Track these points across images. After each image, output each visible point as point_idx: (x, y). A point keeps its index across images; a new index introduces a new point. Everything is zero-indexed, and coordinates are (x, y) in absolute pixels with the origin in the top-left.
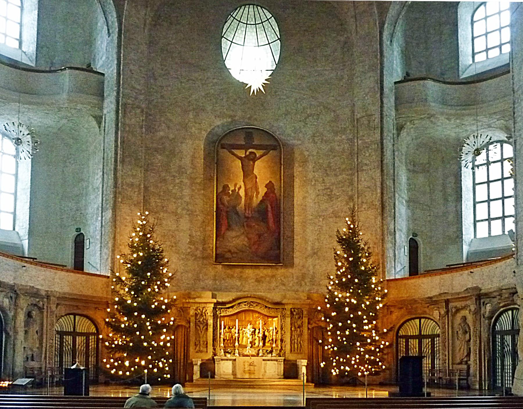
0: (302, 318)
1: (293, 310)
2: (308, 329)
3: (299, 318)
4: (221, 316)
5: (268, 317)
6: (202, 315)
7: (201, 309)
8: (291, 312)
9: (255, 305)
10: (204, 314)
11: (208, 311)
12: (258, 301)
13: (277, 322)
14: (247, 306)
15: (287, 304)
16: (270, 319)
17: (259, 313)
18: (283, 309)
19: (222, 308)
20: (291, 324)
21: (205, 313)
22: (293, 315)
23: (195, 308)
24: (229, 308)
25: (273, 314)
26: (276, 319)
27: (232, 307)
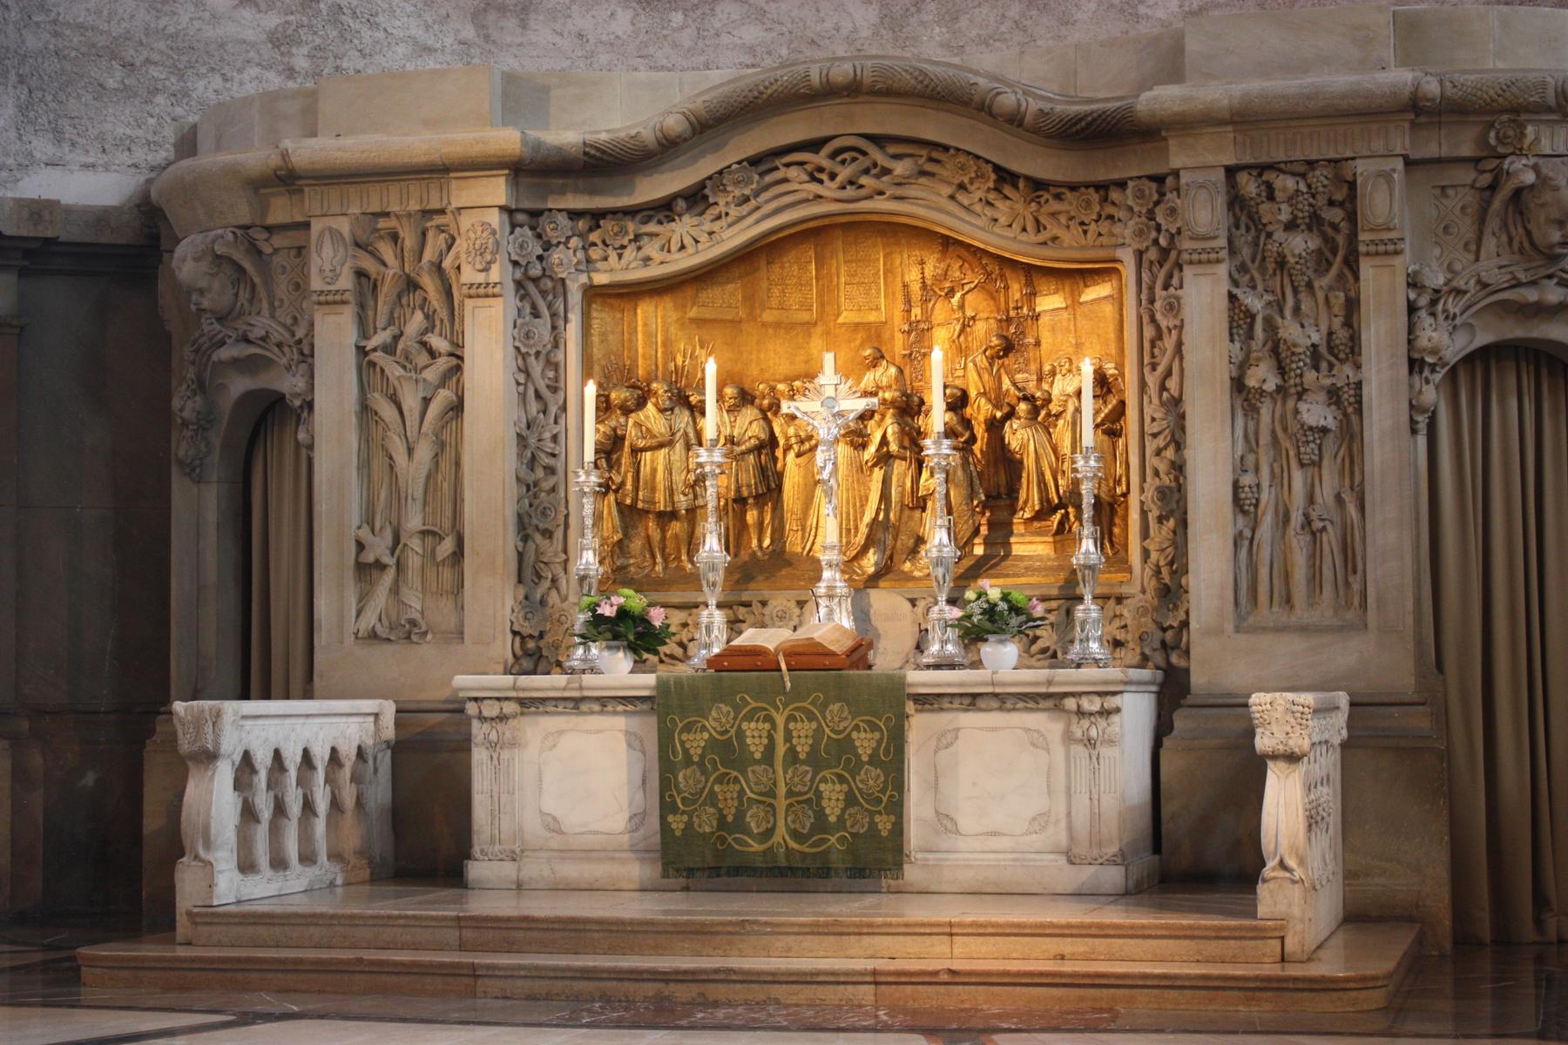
0: (1351, 263)
1: (1249, 186)
2: (1415, 365)
3: (1322, 261)
4: (593, 294)
5: (1031, 273)
6: (412, 285)
7: (409, 241)
8: (1236, 202)
9: (900, 168)
10: (429, 283)
11: (461, 245)
12: (930, 127)
13: (1109, 309)
14: (829, 189)
15: (1188, 124)
16: (1050, 301)
17: (948, 244)
18: (1159, 179)
19: (597, 217)
20: (1239, 320)
21: (438, 268)
22: (1256, 223)
23: (344, 226)
24: (665, 209)
25: (1072, 245)
26: (1096, 292)
27: (696, 198)
